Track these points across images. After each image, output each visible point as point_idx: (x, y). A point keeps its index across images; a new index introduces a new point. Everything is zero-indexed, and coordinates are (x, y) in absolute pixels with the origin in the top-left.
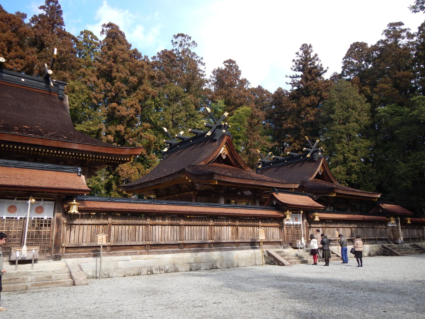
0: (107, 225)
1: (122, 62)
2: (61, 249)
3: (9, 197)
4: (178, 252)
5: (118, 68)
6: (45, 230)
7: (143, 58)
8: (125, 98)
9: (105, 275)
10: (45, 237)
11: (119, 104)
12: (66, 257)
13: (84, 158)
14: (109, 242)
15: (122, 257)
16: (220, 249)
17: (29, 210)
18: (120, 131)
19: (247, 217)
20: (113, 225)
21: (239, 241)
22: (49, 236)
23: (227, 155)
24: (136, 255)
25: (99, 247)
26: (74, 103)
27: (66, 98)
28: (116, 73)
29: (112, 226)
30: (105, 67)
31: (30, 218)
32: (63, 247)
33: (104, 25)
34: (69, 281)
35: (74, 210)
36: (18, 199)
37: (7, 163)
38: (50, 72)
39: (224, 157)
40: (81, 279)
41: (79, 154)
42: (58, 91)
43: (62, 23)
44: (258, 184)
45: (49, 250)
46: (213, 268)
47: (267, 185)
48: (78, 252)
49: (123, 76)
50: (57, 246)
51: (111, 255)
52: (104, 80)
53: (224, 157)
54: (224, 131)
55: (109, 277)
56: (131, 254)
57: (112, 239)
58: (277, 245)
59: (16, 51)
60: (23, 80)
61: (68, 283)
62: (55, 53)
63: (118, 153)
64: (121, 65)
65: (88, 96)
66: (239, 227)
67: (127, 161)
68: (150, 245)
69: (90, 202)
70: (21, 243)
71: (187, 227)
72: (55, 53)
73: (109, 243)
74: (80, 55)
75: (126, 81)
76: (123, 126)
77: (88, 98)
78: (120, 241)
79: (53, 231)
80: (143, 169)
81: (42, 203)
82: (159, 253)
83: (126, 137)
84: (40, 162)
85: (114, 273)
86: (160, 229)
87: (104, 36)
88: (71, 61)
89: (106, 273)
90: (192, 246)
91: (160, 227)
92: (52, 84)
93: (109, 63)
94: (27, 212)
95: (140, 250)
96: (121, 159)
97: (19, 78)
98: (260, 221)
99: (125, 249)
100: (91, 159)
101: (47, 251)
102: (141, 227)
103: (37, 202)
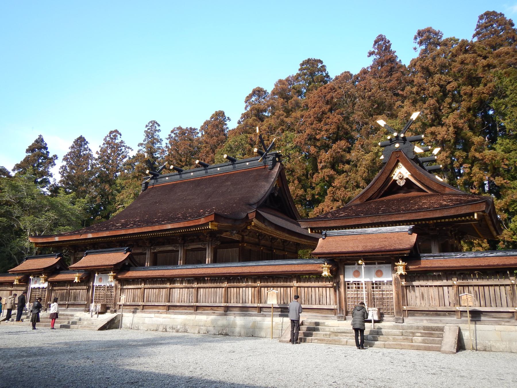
4: (191, 314)
16: (234, 314)
19: (312, 274)
21: (261, 305)
23: (407, 180)
33: (416, 38)
39: (402, 183)
44: (380, 221)
46: (222, 334)
47: (400, 219)
50: (115, 304)
51: (145, 312)
53: (402, 183)
54: (397, 145)
55: (138, 329)
58: (328, 313)
60: (247, 164)
63: (197, 224)
66: (262, 289)
68: (169, 306)
71: (202, 290)
82: (175, 313)
86: (178, 291)
90: (207, 308)
91: (179, 289)
95: (163, 309)
98: (295, 279)
102: (164, 290)
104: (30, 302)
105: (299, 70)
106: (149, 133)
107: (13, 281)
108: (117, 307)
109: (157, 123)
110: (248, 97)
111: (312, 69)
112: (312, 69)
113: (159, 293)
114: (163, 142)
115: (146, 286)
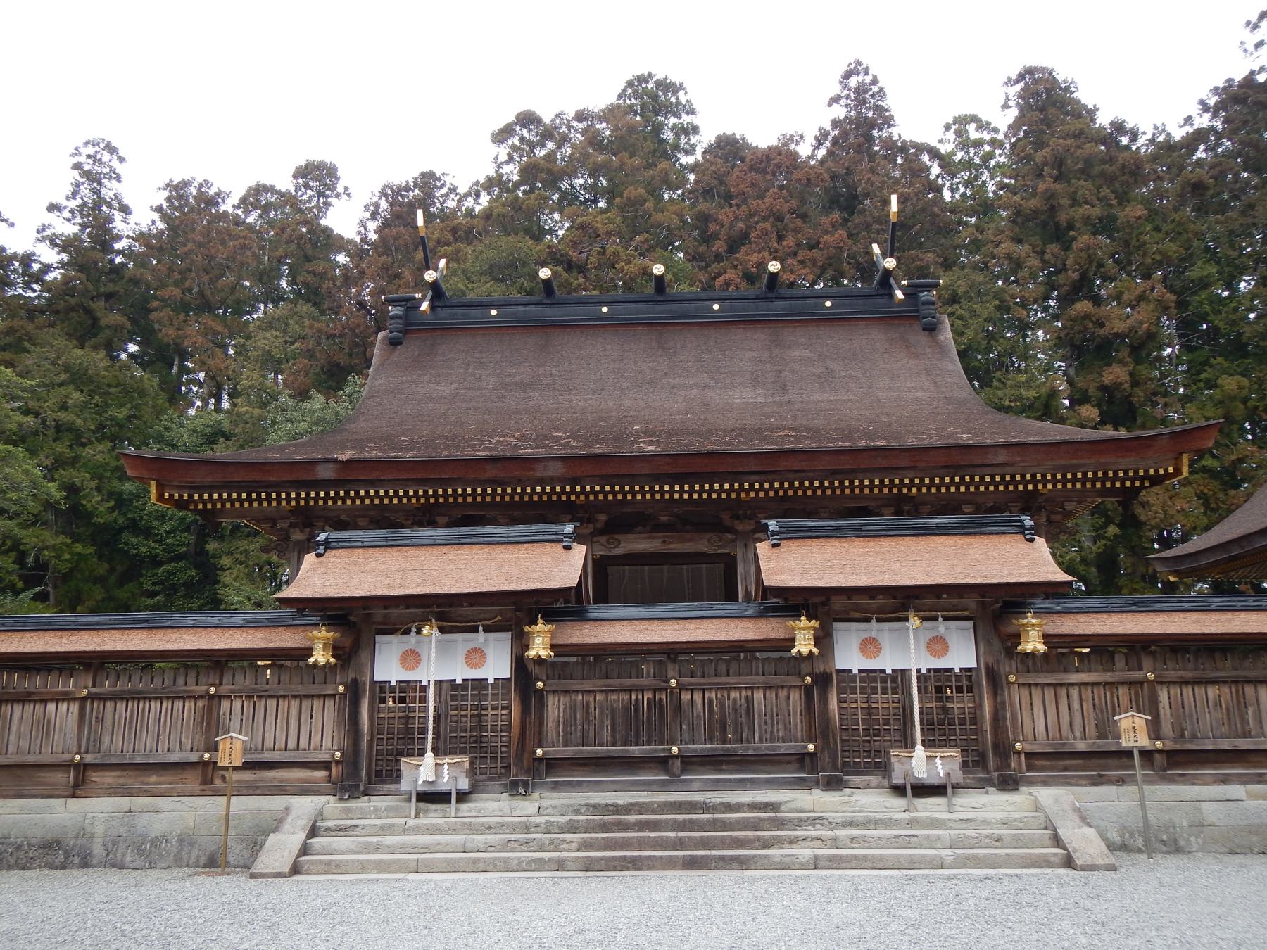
0: (1141, 683)
1: (1082, 171)
2: (1014, 758)
3: (857, 615)
5: (1075, 192)
6: (960, 704)
7: (1149, 136)
8: (1112, 279)
9: (1164, 842)
10: (962, 722)
11: (1097, 301)
12: (1031, 782)
13: (1030, 487)
14: (1158, 738)
15: (1210, 788)
17: (912, 647)
18: (1117, 386)
20: (1162, 683)
22: (974, 721)
24: (1259, 782)
25: (1128, 753)
26: (962, 334)
27: (941, 322)
28: (1071, 211)
29: (1158, 687)
30: (1033, 203)
31: (919, 670)
32: (1019, 753)
33: (1010, 82)
34: (1055, 855)
35: (1033, 643)
36: (878, 620)
37: (838, 529)
38: (890, 263)
40: (1092, 851)
41: (1013, 477)
42: (917, 311)
43: (889, 121)
45: (981, 761)
48: (1066, 769)
49: (1096, 212)
50: (1003, 751)
51: (1171, 780)
52: (1037, 241)
56: (1243, 780)
57: (1166, 727)
59: (795, 231)
60: (828, 304)
61: (1053, 859)
62: (894, 207)
64: (1082, 182)
65: (997, 302)
67: (1167, 476)
69: (1073, 616)
70: (906, 739)
72: (894, 207)
73: (1159, 744)
74: (952, 190)
75: (1105, 225)
76: (1125, 364)
77: (998, 308)
78: (1194, 736)
79: (981, 705)
80: (1221, 496)
81: (941, 627)
83: (1139, 396)
84: (909, 513)
85: (1193, 839)
87: (1013, 113)
88: (934, 216)
89: (1165, 837)
92: (899, 295)
93: (1041, 187)
94: (906, 651)
96: (1146, 472)
97: (819, 301)
99: (1216, 762)
100: (1050, 486)
101: (976, 763)
103: (927, 624)
104: (436, 751)
105: (620, 96)
106: (88, 175)
107: (308, 651)
108: (1017, 764)
109: (111, 149)
110: (502, 131)
111: (652, 102)
112: (652, 102)
113: (1242, 704)
114: (132, 219)
115: (1172, 674)
